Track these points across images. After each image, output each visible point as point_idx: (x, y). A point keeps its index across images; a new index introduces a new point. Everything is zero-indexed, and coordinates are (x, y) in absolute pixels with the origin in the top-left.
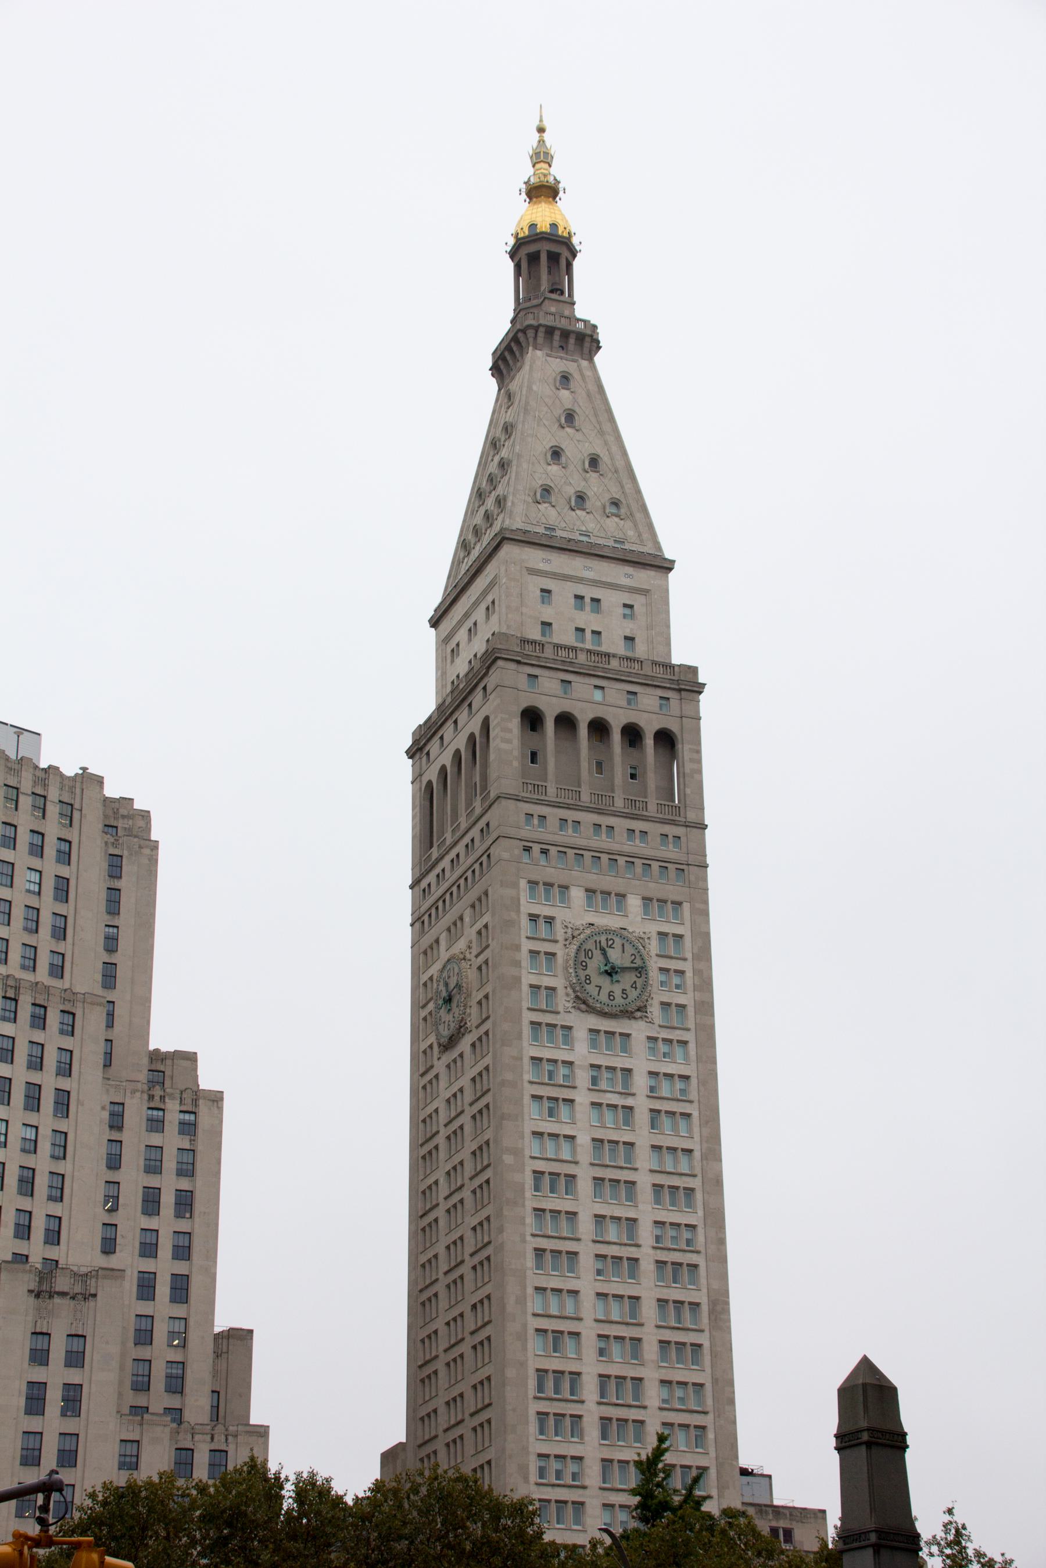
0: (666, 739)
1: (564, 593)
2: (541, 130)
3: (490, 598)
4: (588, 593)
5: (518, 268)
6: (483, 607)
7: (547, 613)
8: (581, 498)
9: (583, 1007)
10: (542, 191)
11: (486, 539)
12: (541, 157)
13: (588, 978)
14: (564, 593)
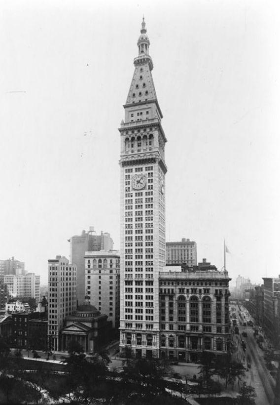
1: (135, 114)
2: (143, 19)
4: (140, 112)
8: (140, 94)
10: (144, 31)
12: (143, 24)
14: (135, 114)
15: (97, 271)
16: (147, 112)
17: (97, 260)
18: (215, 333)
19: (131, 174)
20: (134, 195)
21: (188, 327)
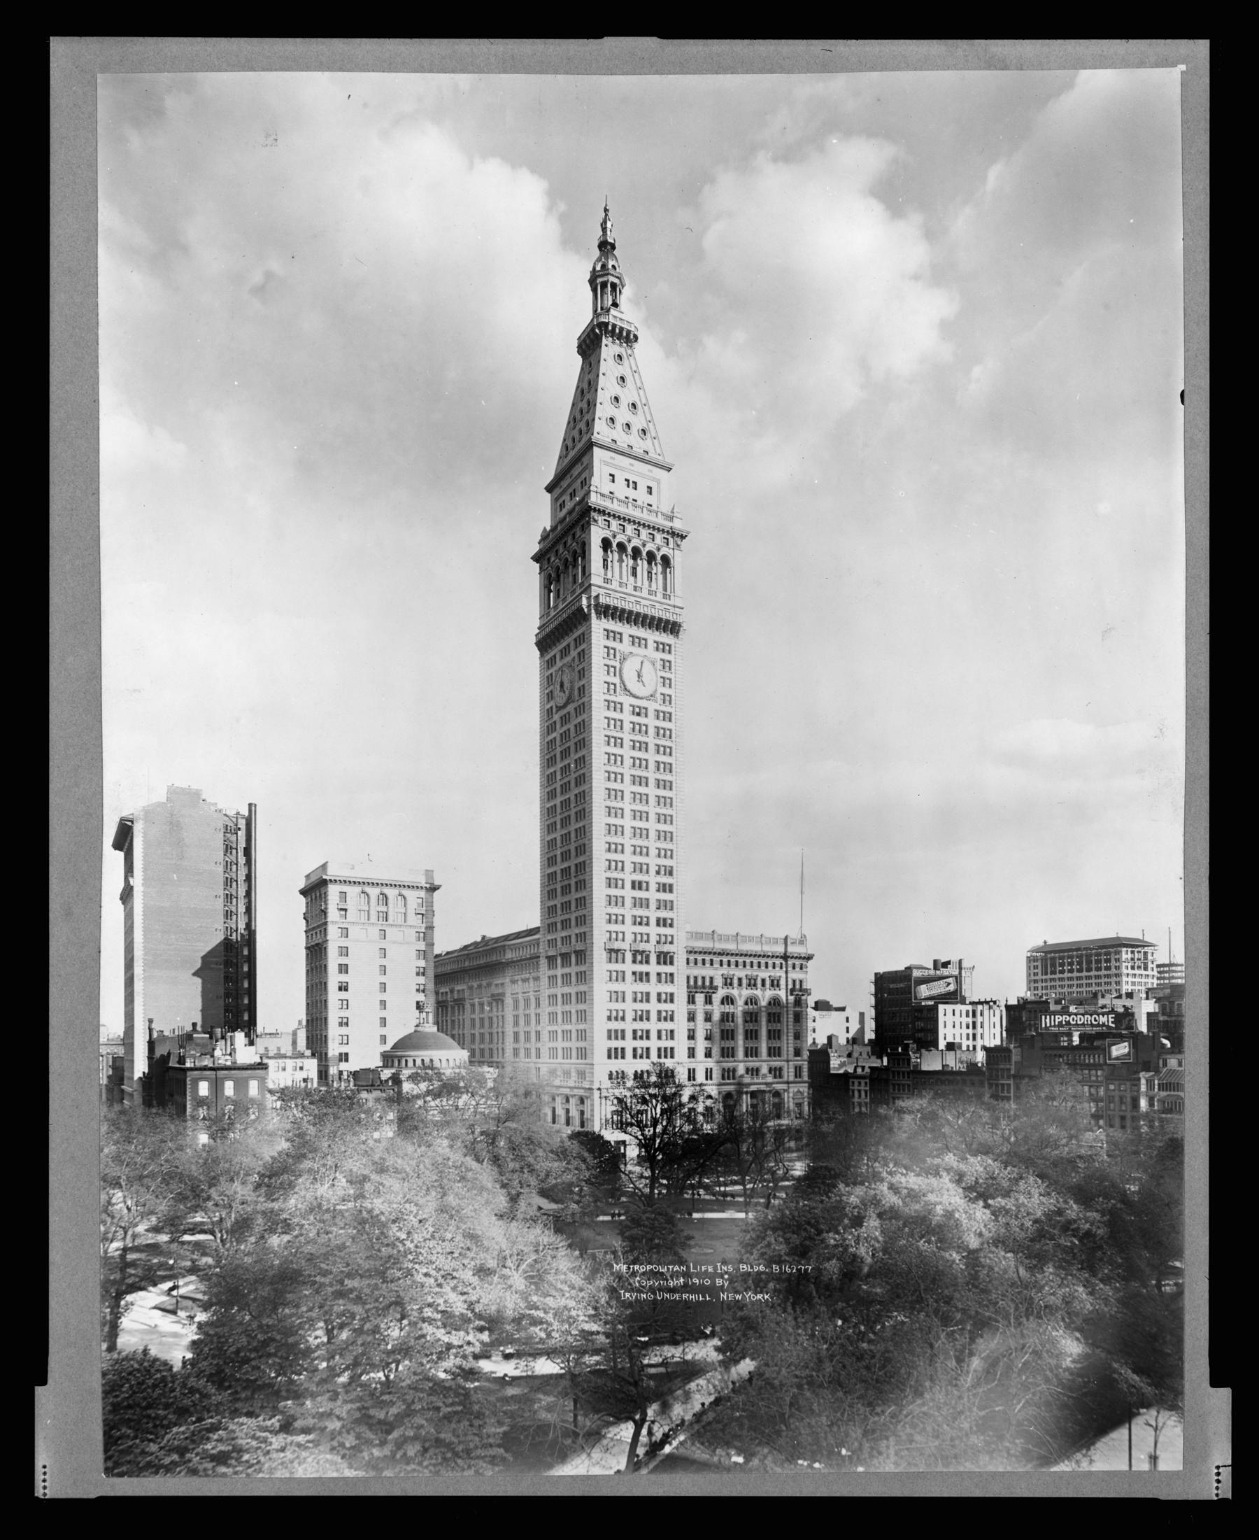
0: (666, 561)
2: (606, 210)
3: (583, 476)
5: (594, 290)
6: (579, 481)
11: (579, 446)
15: (374, 932)
17: (374, 892)
18: (792, 1078)
21: (741, 1070)
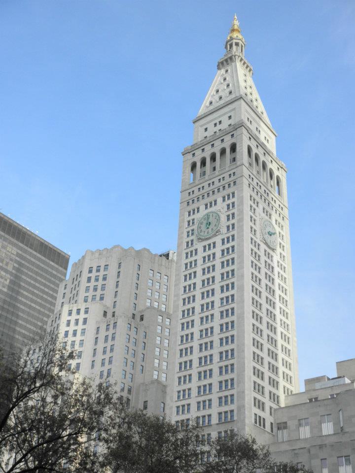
1: (211, 127)
4: (217, 121)
7: (206, 134)
9: (200, 240)
13: (201, 231)
14: (211, 127)
16: (230, 117)
19: (197, 216)
20: (200, 250)
